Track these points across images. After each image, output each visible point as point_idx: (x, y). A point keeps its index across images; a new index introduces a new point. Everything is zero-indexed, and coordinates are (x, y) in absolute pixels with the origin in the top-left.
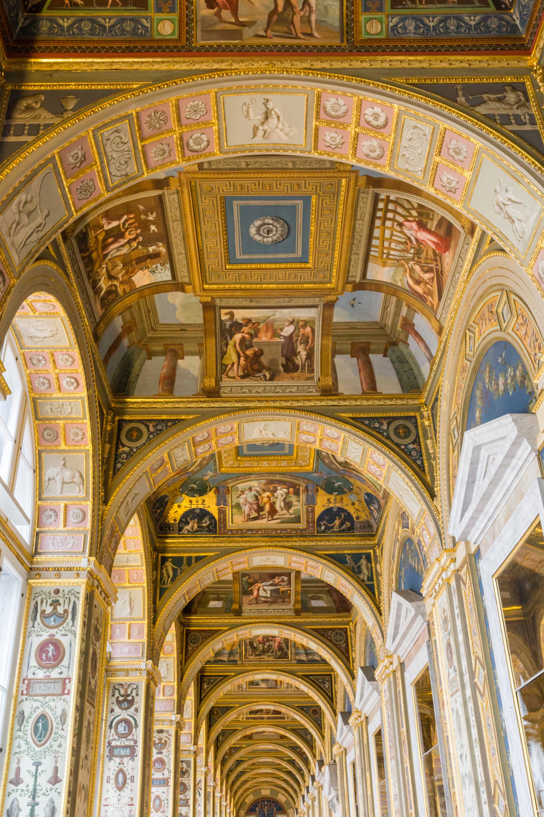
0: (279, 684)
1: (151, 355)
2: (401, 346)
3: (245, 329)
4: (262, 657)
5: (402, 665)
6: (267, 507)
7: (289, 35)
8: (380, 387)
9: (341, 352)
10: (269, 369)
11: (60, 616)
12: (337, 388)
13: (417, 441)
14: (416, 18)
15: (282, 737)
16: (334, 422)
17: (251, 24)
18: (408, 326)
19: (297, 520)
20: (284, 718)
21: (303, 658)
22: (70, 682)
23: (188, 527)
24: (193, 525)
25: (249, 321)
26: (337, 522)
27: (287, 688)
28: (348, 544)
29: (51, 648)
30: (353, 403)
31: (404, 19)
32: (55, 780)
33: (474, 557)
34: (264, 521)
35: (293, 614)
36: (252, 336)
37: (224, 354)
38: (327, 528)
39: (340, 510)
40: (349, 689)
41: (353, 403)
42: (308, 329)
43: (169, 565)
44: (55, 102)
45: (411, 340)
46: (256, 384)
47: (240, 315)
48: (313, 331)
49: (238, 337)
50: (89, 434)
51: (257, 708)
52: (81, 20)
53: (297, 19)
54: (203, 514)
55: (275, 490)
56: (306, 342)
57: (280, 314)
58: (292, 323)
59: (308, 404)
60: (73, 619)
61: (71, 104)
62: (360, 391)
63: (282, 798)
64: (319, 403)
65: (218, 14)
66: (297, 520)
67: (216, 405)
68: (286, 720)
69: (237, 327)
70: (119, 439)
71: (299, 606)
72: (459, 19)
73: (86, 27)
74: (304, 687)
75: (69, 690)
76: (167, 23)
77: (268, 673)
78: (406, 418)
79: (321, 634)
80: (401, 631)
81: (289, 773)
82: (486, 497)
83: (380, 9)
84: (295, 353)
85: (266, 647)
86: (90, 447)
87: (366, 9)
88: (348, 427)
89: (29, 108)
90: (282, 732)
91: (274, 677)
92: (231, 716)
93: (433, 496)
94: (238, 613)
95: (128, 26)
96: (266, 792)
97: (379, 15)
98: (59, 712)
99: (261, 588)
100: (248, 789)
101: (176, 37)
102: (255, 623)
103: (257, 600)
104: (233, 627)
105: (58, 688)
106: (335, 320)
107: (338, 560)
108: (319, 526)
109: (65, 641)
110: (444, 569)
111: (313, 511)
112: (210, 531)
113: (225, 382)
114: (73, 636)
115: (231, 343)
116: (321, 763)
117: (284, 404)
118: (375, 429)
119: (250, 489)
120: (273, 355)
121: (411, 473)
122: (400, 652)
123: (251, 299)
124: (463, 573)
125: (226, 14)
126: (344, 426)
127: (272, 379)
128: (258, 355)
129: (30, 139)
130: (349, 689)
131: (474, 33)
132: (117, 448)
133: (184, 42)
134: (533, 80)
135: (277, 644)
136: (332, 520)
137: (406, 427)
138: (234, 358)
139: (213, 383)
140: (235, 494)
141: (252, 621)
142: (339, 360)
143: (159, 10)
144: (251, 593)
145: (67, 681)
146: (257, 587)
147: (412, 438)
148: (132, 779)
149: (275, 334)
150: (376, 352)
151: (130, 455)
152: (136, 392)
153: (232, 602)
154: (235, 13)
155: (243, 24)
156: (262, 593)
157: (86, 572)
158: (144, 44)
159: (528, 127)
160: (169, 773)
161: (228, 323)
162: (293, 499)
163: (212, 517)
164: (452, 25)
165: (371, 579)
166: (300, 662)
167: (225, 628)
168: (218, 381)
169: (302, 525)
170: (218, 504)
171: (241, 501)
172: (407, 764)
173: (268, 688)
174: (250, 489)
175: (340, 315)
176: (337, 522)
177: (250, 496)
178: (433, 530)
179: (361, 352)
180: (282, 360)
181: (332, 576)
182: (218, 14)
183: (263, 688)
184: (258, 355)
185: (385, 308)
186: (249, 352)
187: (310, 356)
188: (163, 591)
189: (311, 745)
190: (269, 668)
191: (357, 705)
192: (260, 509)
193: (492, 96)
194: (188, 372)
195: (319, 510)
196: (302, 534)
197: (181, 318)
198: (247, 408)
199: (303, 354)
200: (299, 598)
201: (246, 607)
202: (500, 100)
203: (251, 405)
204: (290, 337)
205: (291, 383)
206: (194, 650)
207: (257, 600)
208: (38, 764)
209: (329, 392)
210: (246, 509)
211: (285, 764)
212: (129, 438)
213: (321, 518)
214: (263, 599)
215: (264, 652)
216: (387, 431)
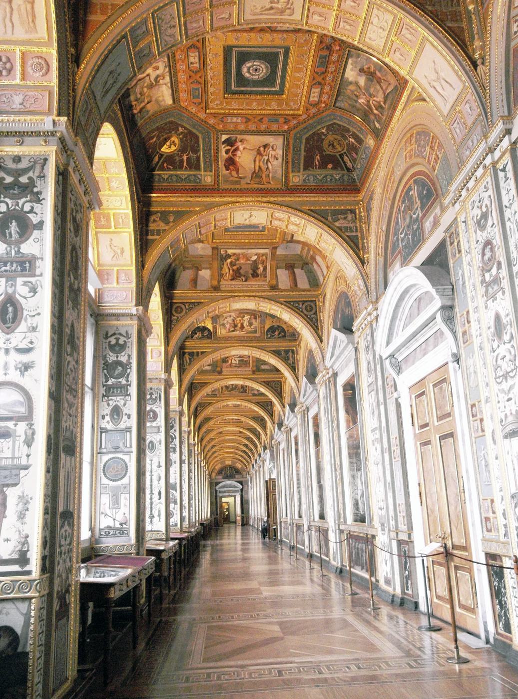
1: (185, 268)
2: (310, 265)
3: (233, 257)
5: (307, 408)
6: (239, 325)
7: (260, 183)
8: (300, 285)
9: (280, 268)
10: (244, 276)
11: (154, 400)
12: (278, 286)
13: (315, 313)
14: (313, 175)
15: (241, 432)
16: (276, 304)
17: (244, 178)
18: (313, 259)
19: (255, 332)
21: (256, 392)
23: (196, 336)
24: (199, 335)
25: (235, 254)
26: (277, 333)
28: (282, 345)
29: (151, 414)
30: (286, 293)
31: (308, 176)
32: (159, 466)
33: (335, 375)
34: (238, 332)
35: (251, 373)
36: (236, 260)
37: (222, 268)
38: (272, 336)
39: (279, 326)
40: (281, 413)
41: (286, 293)
42: (264, 257)
43: (187, 356)
44: (164, 216)
45: (314, 264)
46: (238, 284)
47: (230, 252)
48: (267, 258)
49: (229, 261)
50: (161, 317)
52: (172, 175)
53: (264, 176)
54: (205, 329)
55: (244, 317)
56: (263, 263)
57: (250, 251)
58: (256, 255)
59: (263, 294)
60: (160, 400)
61: (171, 219)
62: (289, 288)
63: (239, 466)
64: (269, 294)
65: (230, 173)
66: (255, 332)
67: (219, 294)
69: (229, 256)
70: (171, 313)
71: (254, 369)
72: (332, 176)
73: (174, 178)
74: (256, 408)
76: (209, 177)
78: (311, 301)
79: (267, 384)
80: (307, 394)
81: (244, 452)
82: (341, 353)
83: (299, 172)
84: (258, 268)
86: (162, 323)
87: (293, 171)
88: (283, 306)
89: (154, 221)
90: (241, 430)
91: (238, 403)
92: (212, 423)
93: (321, 341)
94: (220, 373)
95: (192, 178)
96: (228, 462)
97: (298, 174)
98: (158, 440)
101: (213, 183)
103: (231, 365)
104: (217, 381)
105: (156, 430)
106: (278, 253)
107: (277, 353)
108: (267, 335)
109: (157, 410)
110: (324, 376)
111: (264, 327)
112: (208, 338)
113: (223, 283)
115: (225, 263)
116: (265, 448)
117: (252, 294)
118: (296, 307)
119: (230, 316)
120: (246, 269)
121: (312, 330)
122: (307, 403)
123: (236, 246)
124: (331, 379)
125: (234, 173)
126: (281, 305)
127: (246, 281)
128: (239, 269)
129: (157, 237)
130: (281, 413)
131: (338, 183)
132: (171, 317)
133: (216, 186)
134: (359, 208)
136: (274, 332)
137: (311, 306)
138: (227, 270)
139: (216, 283)
140: (222, 319)
142: (279, 271)
143: (205, 171)
144: (228, 361)
147: (313, 311)
148: (175, 462)
149: (248, 259)
150: (297, 268)
151: (177, 321)
152: (178, 288)
153: (217, 367)
154: (237, 173)
155: (241, 178)
156: (233, 362)
158: (199, 189)
159: (354, 234)
160: (185, 457)
161: (224, 255)
162: (254, 321)
163: (209, 330)
164: (329, 178)
165: (294, 363)
166: (254, 395)
168: (219, 282)
169: (258, 335)
170: (212, 324)
171: (225, 322)
172: (308, 454)
174: (230, 316)
175: (279, 252)
176: (277, 333)
177: (230, 320)
178: (321, 357)
179: (290, 267)
180: (251, 272)
181: (273, 361)
182: (230, 173)
184: (239, 269)
185: (302, 250)
186: (235, 268)
187: (265, 269)
188: (184, 370)
189: (258, 437)
191: (285, 422)
192: (235, 326)
193: (342, 216)
194: (204, 277)
195: (267, 327)
196: (258, 340)
197: (201, 253)
198: (232, 297)
199: (262, 269)
200: (255, 364)
201: (224, 370)
202: (345, 218)
203: (236, 294)
204: (255, 260)
205: (255, 283)
206: (195, 393)
207: (231, 365)
208: (151, 461)
209: (274, 288)
210: (228, 326)
211: (241, 447)
212: (176, 312)
213: (268, 331)
215: (232, 389)
216: (302, 308)
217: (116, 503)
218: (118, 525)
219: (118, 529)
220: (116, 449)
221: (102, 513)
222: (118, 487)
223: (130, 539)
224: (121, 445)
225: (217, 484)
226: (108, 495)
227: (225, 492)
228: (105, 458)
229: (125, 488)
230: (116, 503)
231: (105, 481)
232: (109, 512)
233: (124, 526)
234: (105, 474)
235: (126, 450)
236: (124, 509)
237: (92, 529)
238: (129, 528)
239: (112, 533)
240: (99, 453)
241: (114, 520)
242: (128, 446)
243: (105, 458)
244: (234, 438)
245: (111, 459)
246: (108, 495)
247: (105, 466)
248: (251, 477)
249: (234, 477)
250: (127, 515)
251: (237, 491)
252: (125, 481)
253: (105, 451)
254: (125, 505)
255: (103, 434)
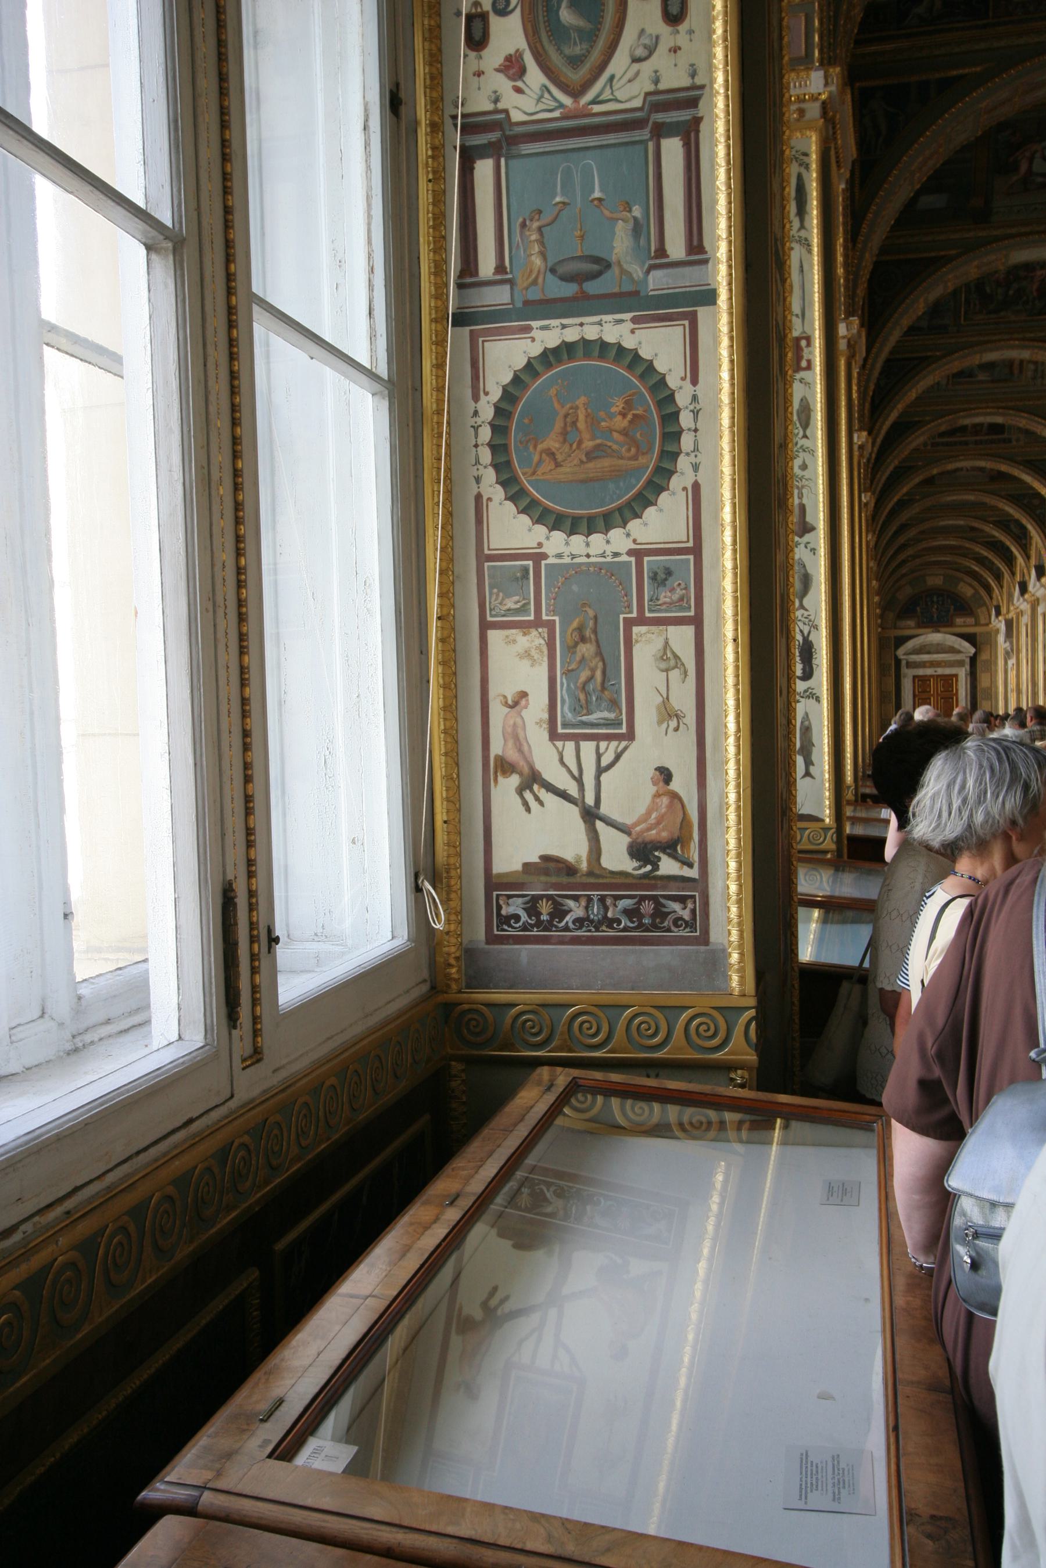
0: (1016, 372)
4: (1002, 314)
15: (1000, 477)
20: (1010, 441)
22: (809, 345)
27: (1034, 378)
51: (967, 422)
63: (966, 589)
68: (1014, 443)
75: (809, 362)
77: (1013, 347)
85: (1011, 292)
96: (935, 581)
99: (1038, 155)
100: (904, 576)
102: (1020, 235)
114: (804, 251)
135: (1035, 287)
141: (1014, 231)
145: (803, 343)
146: (1028, 154)
157: (817, 105)
167: (953, 252)
173: (993, 381)
183: (981, 382)
190: (1016, 336)
214: (1040, 180)
217: (596, 700)
218: (616, 857)
219: (619, 881)
220: (586, 283)
221: (505, 767)
222: (609, 571)
223: (716, 961)
224: (621, 245)
225: (901, 641)
226: (535, 640)
227: (923, 665)
228: (506, 356)
229: (662, 578)
230: (596, 700)
231: (511, 529)
232: (545, 757)
233: (668, 866)
234: (503, 468)
235: (658, 282)
236: (655, 745)
237: (430, 867)
238: (702, 883)
239: (577, 910)
240: (461, 319)
241: (590, 815)
242: (676, 248)
243: (506, 356)
244: (971, 497)
245: (550, 357)
246: (535, 640)
247: (500, 411)
248: (1009, 624)
249: (950, 624)
250: (683, 784)
251: (960, 664)
252: (661, 524)
253: (499, 297)
254: (668, 713)
255: (484, 169)
